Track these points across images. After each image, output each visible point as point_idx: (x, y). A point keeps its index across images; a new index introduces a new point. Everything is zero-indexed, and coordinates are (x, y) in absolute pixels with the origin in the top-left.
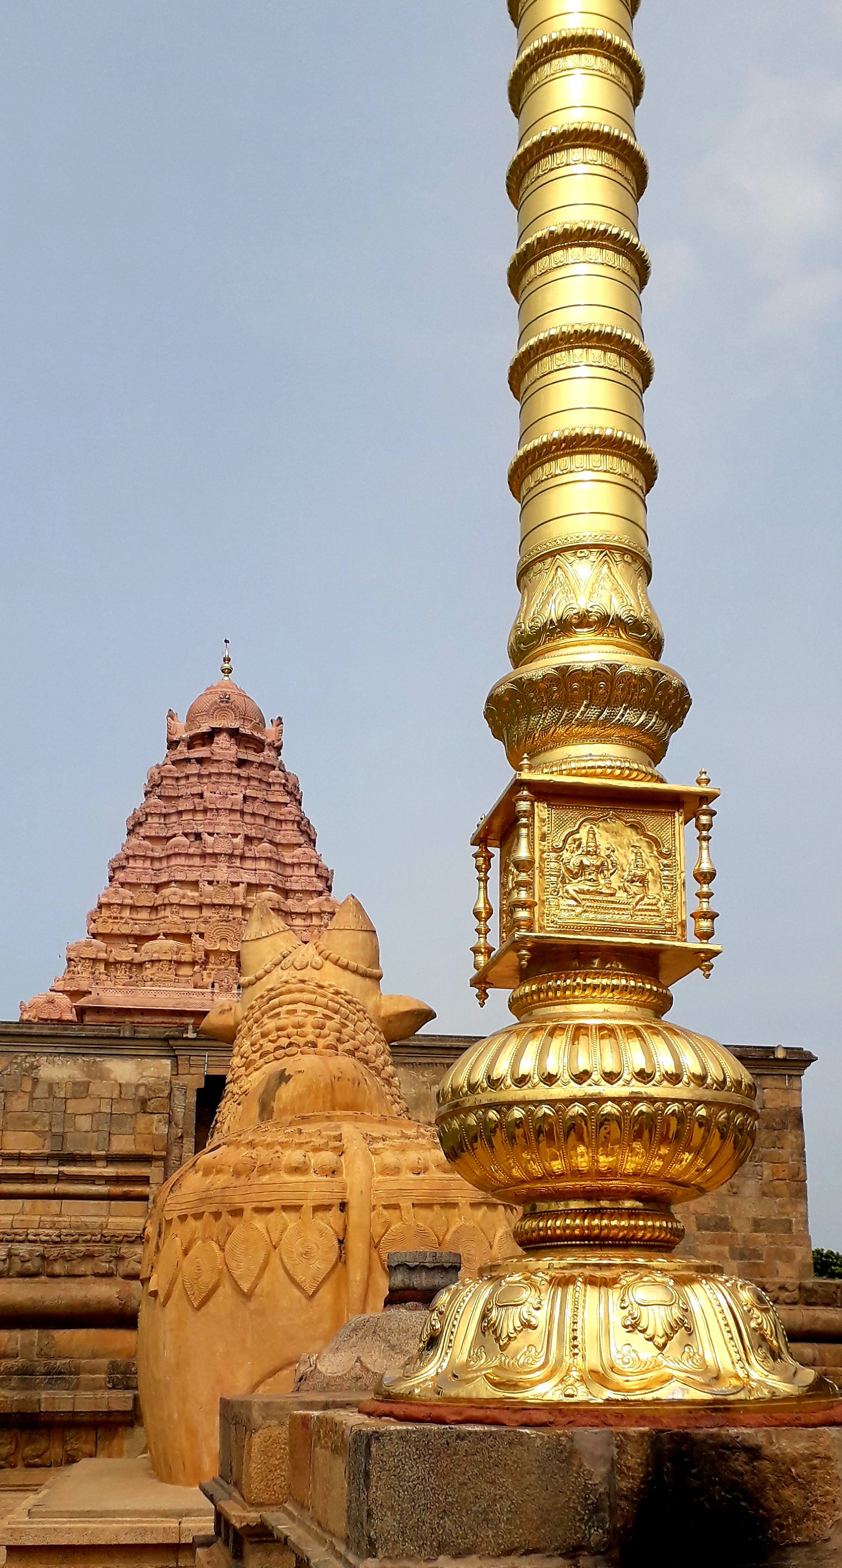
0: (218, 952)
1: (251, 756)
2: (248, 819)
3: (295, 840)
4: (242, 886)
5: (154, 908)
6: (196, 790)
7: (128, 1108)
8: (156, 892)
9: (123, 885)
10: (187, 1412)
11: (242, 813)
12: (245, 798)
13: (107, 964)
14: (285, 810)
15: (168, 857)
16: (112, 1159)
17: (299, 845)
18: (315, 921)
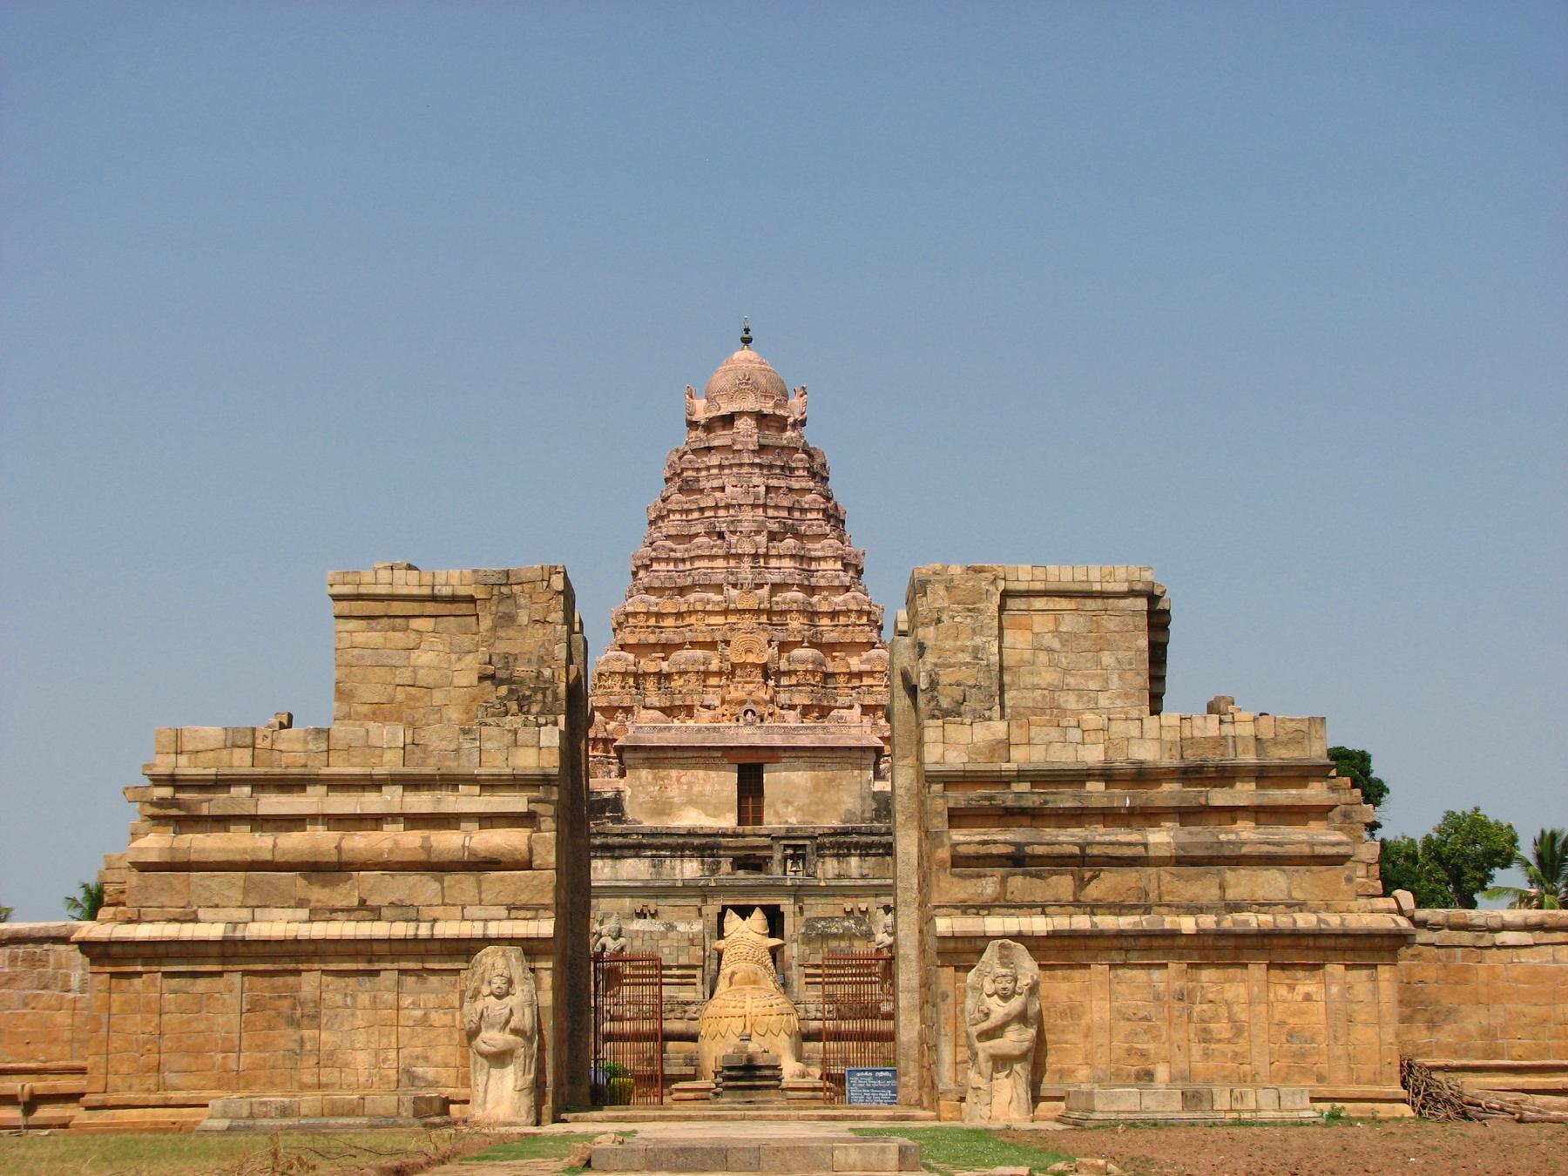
0: (744, 665)
1: (771, 438)
2: (771, 513)
3: (819, 531)
4: (767, 588)
5: (679, 615)
6: (716, 483)
7: (686, 943)
8: (682, 595)
9: (648, 590)
10: (710, 1065)
11: (765, 506)
12: (768, 488)
13: (636, 675)
14: (809, 497)
15: (692, 559)
16: (679, 967)
17: (825, 536)
18: (842, 620)
